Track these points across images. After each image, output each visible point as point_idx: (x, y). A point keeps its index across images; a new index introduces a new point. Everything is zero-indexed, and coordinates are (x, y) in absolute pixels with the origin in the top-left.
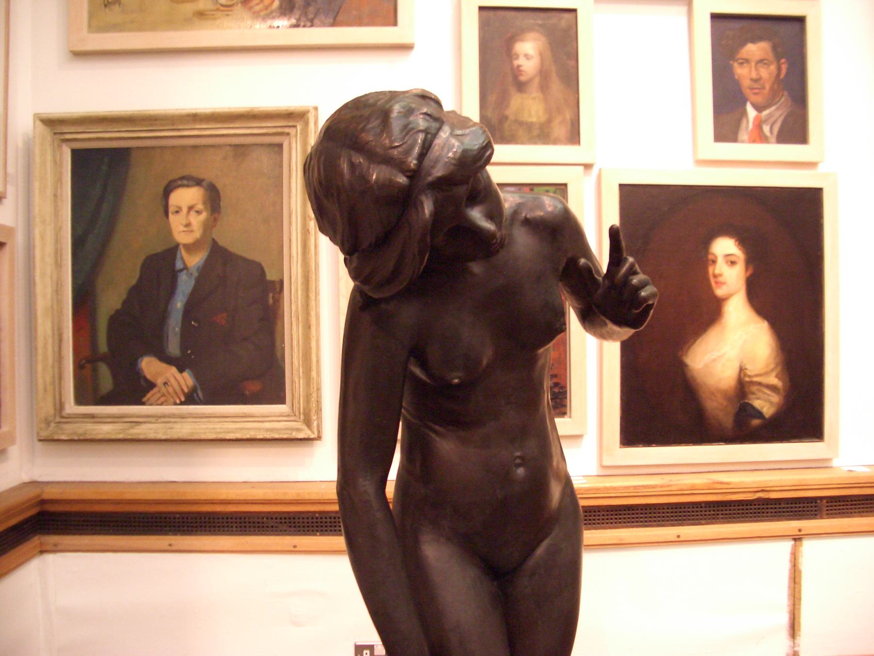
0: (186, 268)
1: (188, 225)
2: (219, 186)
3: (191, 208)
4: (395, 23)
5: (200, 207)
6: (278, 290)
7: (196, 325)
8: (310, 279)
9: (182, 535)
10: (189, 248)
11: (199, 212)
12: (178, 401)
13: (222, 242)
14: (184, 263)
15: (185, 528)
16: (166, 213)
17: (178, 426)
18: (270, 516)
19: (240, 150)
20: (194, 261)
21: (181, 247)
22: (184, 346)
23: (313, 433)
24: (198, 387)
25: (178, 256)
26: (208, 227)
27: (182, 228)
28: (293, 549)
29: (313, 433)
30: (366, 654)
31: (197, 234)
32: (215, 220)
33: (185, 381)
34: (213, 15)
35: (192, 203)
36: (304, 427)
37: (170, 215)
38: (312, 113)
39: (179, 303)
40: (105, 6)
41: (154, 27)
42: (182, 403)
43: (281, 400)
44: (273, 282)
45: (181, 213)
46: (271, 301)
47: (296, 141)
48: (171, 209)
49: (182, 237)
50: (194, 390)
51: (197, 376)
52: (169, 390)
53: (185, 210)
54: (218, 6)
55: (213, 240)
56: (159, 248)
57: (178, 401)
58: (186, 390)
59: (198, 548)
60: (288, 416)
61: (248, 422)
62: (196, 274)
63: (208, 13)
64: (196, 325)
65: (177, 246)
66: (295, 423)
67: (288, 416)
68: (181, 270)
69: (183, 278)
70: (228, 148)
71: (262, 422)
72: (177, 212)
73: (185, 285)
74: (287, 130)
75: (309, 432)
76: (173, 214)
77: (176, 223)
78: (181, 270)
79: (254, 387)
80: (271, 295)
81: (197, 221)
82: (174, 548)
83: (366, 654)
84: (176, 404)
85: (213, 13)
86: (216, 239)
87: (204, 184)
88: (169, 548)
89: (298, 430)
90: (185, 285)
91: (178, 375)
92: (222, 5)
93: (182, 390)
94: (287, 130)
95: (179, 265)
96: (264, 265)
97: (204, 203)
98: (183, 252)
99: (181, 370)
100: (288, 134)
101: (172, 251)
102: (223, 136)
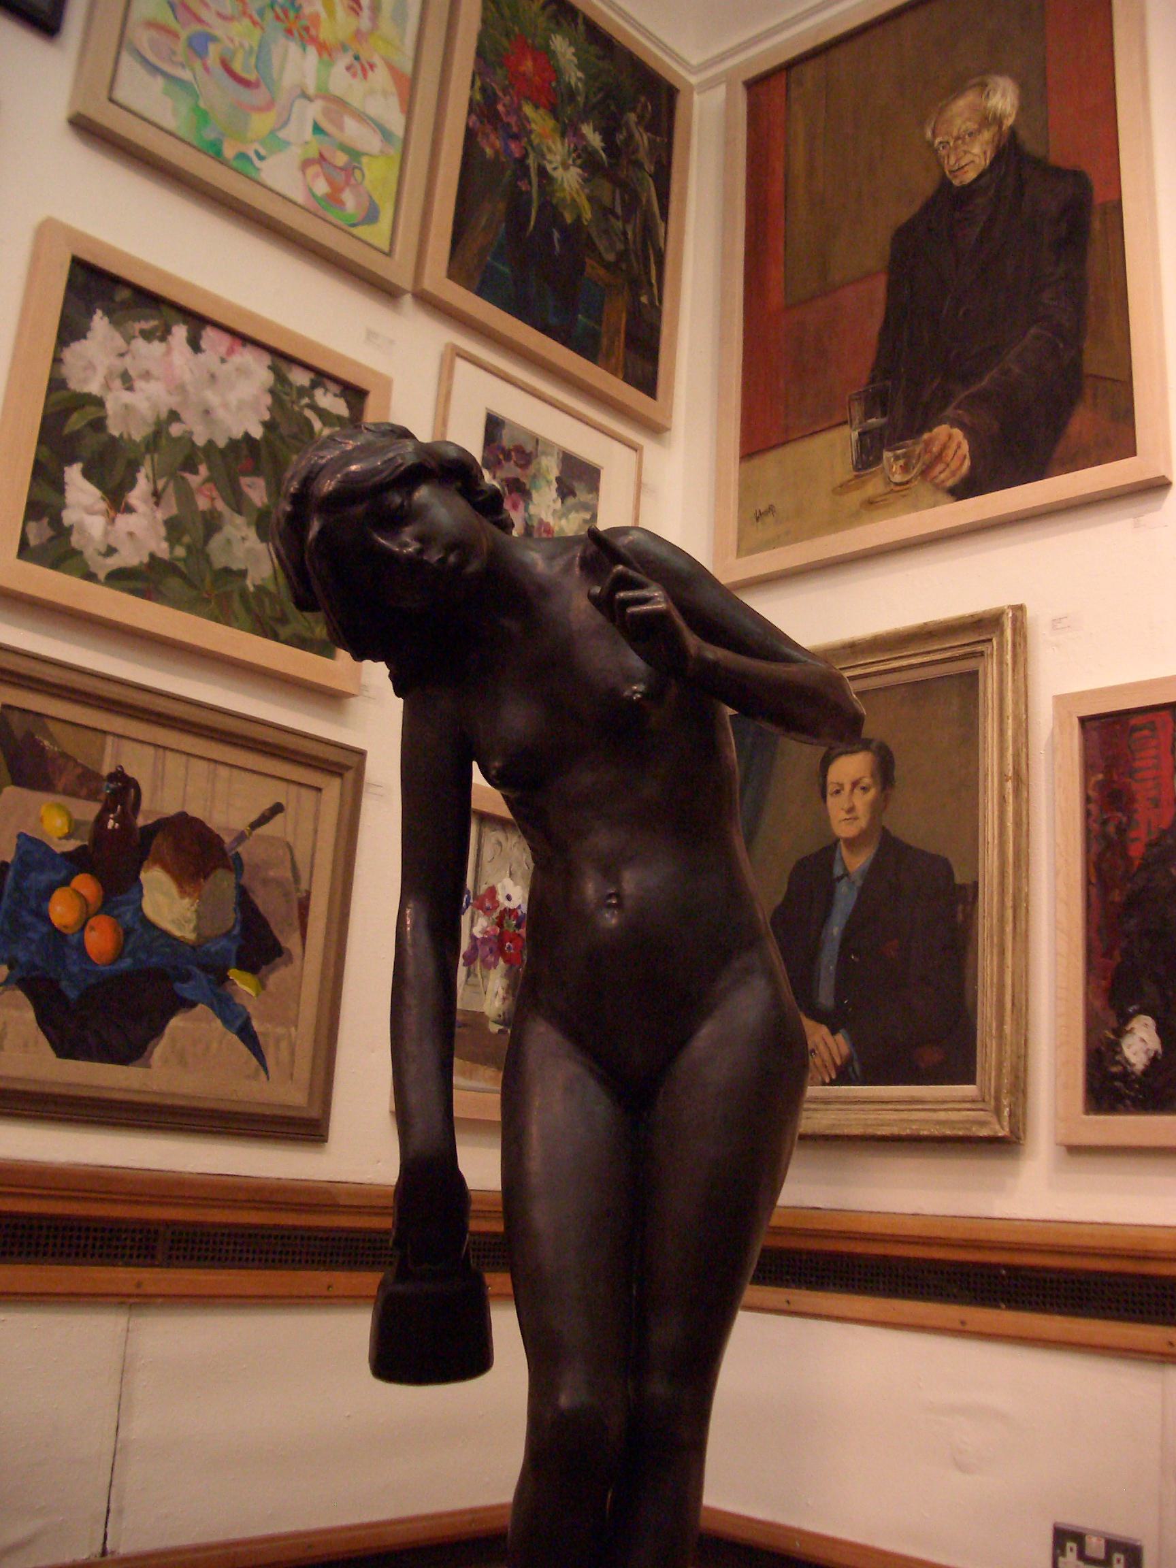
0: (846, 874)
1: (851, 810)
2: (892, 746)
3: (855, 784)
4: (1135, 454)
5: (867, 781)
6: (970, 900)
7: (857, 960)
8: (1006, 875)
9: (807, 1289)
10: (852, 843)
11: (865, 789)
12: (827, 1080)
13: (897, 830)
14: (845, 869)
15: (813, 1279)
16: (824, 797)
17: (818, 1115)
18: (936, 1267)
19: (920, 690)
20: (857, 862)
21: (841, 842)
22: (839, 993)
23: (1002, 1128)
24: (855, 1057)
25: (837, 856)
26: (878, 808)
27: (844, 815)
28: (959, 1327)
29: (1002, 1128)
30: (1119, 1561)
31: (863, 822)
32: (886, 799)
33: (838, 1048)
34: (885, 500)
35: (858, 776)
36: (993, 1119)
37: (829, 797)
38: (1008, 614)
39: (836, 929)
40: (757, 519)
41: (814, 532)
42: (833, 1083)
43: (971, 1081)
44: (963, 887)
45: (842, 792)
46: (960, 917)
47: (992, 664)
48: (831, 788)
49: (844, 830)
50: (848, 1061)
51: (855, 1041)
52: (817, 1063)
53: (847, 788)
54: (892, 486)
55: (883, 828)
56: (810, 847)
57: (827, 1080)
58: (838, 1062)
59: (824, 1312)
60: (973, 1101)
61: (916, 1110)
62: (859, 883)
63: (877, 500)
64: (857, 960)
65: (836, 842)
66: (982, 1113)
67: (973, 1101)
68: (841, 878)
69: (842, 888)
70: (68, 354)
71: (934, 1110)
72: (838, 792)
73: (845, 899)
74: (979, 648)
75: (998, 1127)
76: (832, 795)
77: (836, 806)
78: (841, 878)
79: (931, 1056)
80: (960, 907)
81: (862, 802)
82: (792, 1308)
83: (1119, 1561)
84: (824, 1084)
85: (883, 498)
86: (887, 827)
87: (874, 745)
88: (785, 1306)
89: (982, 1124)
90: (845, 899)
91: (829, 1039)
92: (897, 484)
93: (835, 1064)
94: (979, 648)
95: (838, 871)
96: (952, 860)
97: (872, 776)
98: (844, 851)
99: (834, 1032)
100: (982, 654)
101: (828, 852)
102: (894, 670)
